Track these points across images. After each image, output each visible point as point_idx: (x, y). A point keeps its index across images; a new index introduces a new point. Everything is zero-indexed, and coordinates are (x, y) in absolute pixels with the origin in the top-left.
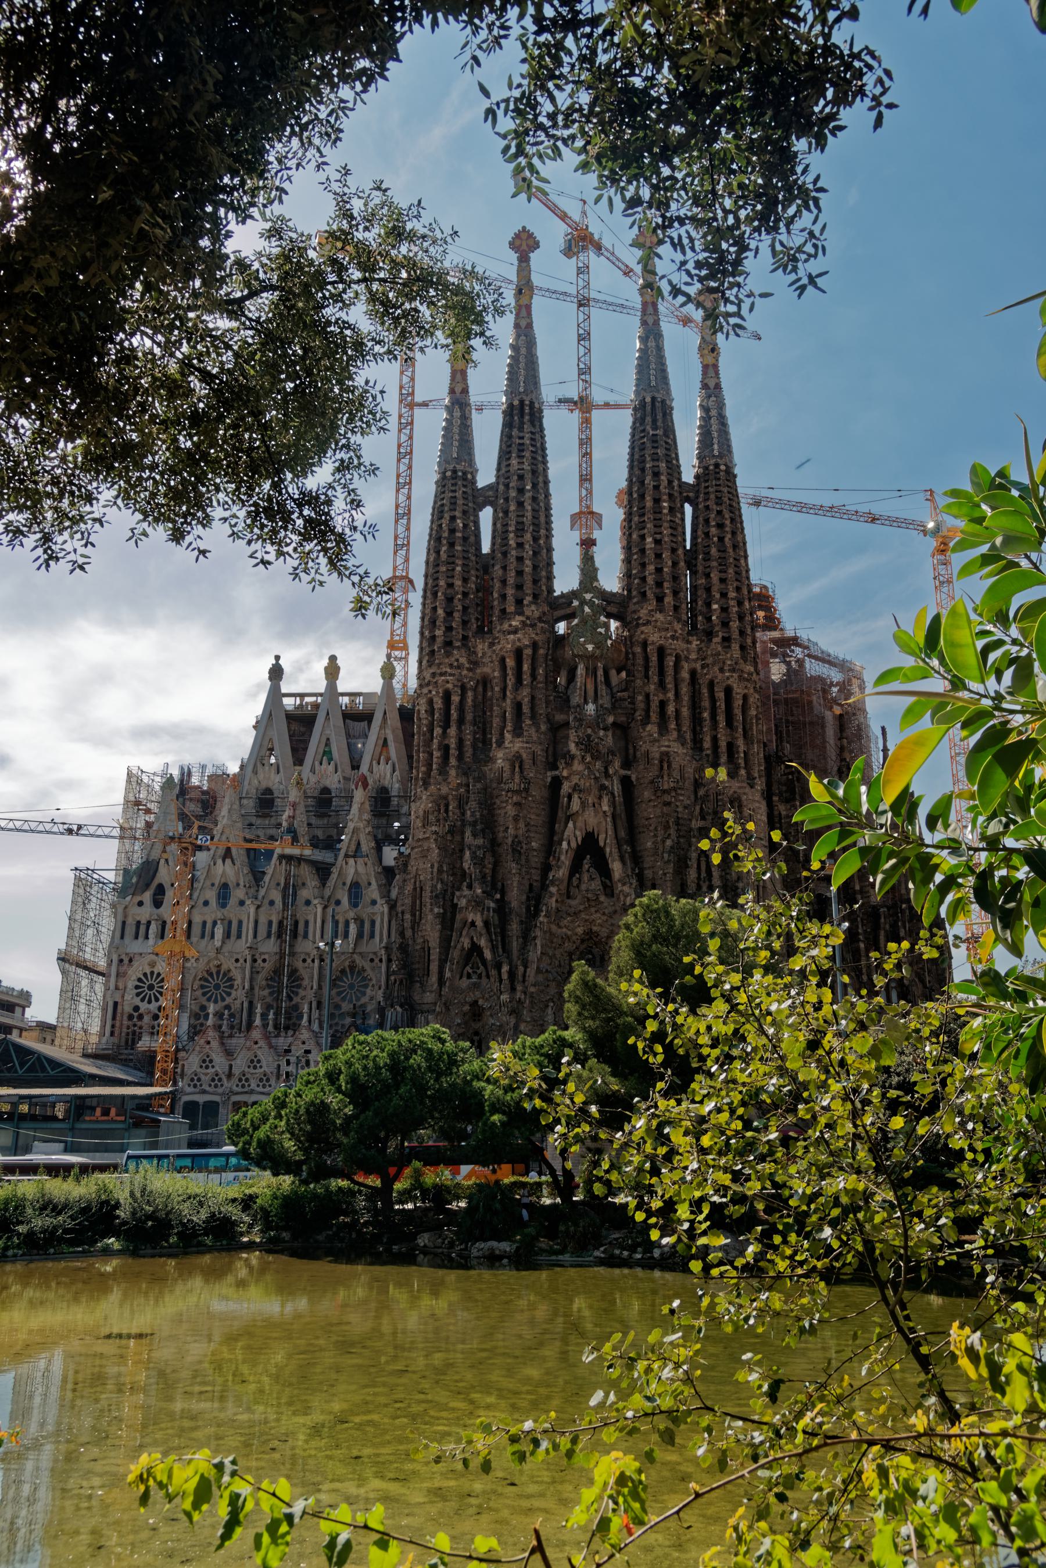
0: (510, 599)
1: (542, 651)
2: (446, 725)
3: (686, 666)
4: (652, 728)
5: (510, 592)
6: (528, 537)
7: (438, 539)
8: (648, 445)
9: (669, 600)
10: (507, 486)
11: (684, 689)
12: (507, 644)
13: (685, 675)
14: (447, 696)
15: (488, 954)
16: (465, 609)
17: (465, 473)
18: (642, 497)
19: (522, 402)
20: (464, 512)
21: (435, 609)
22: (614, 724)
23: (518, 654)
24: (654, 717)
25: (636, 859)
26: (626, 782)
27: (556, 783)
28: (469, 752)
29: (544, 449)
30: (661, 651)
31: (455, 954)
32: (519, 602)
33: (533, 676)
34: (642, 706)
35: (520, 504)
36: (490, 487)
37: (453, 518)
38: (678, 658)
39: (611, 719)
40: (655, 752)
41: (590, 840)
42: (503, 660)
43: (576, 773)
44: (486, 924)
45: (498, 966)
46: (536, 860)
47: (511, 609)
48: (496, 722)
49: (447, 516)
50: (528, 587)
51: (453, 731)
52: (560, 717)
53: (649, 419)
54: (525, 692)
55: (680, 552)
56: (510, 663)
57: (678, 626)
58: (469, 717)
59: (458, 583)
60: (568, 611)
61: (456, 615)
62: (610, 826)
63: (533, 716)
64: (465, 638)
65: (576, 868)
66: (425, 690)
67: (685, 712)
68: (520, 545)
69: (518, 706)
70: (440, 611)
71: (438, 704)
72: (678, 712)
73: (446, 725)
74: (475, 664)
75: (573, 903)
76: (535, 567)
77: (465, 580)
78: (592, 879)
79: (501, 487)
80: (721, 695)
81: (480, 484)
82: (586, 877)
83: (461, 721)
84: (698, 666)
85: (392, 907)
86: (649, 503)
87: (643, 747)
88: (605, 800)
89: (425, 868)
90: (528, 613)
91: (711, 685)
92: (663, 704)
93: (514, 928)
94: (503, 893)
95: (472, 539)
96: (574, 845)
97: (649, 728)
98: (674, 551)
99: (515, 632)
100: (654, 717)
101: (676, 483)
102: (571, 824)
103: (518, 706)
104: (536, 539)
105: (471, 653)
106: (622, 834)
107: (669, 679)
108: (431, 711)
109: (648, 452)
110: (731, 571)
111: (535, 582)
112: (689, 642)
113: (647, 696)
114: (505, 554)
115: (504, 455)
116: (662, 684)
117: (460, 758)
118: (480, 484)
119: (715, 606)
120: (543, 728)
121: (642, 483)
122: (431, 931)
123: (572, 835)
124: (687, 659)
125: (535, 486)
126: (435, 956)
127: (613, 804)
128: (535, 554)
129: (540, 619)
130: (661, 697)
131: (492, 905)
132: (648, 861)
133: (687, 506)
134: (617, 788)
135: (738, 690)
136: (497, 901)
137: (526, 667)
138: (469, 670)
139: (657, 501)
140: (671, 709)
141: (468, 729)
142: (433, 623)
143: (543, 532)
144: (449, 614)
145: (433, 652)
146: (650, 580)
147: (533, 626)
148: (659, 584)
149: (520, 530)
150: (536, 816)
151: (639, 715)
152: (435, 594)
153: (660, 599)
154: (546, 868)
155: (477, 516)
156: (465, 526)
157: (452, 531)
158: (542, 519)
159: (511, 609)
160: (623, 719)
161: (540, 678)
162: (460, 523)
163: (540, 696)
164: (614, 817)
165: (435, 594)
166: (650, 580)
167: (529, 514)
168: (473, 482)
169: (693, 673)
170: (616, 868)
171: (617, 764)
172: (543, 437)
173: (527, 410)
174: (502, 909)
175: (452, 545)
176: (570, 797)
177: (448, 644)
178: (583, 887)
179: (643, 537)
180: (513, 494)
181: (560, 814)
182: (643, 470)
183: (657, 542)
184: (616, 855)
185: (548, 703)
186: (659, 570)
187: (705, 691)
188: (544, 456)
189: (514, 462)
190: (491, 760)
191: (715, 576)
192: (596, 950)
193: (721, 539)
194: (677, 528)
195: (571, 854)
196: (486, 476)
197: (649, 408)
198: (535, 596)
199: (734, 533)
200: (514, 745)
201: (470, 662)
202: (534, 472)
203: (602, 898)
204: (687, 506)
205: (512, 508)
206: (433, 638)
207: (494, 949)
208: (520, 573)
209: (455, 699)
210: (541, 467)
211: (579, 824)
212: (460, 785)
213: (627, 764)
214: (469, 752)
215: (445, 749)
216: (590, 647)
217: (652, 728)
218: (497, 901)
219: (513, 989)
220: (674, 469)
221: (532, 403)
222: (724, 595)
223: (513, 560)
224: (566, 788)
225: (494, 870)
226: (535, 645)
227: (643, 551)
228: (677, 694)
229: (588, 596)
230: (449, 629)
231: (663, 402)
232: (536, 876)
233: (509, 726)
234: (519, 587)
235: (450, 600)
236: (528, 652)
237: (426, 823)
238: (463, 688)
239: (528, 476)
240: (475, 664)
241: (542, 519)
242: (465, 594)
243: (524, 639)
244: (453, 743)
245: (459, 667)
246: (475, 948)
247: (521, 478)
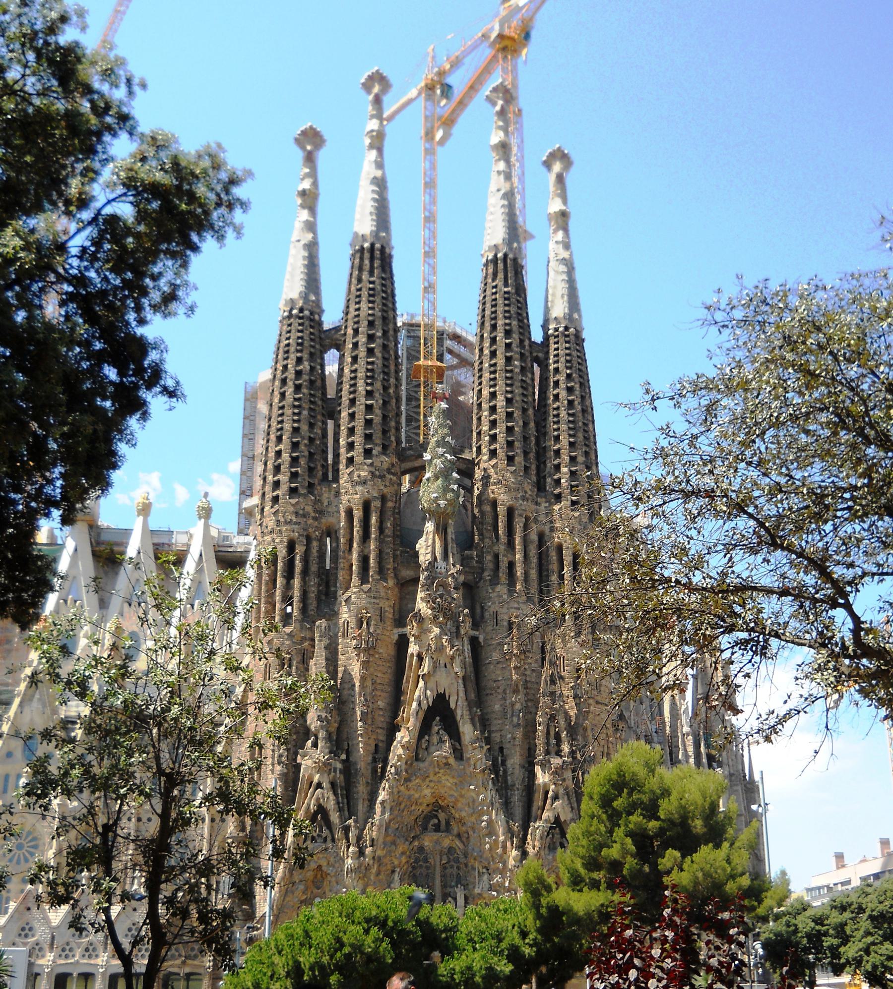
0: (359, 449)
1: (390, 504)
3: (534, 527)
4: (502, 589)
5: (358, 439)
6: (378, 385)
7: (284, 382)
8: (500, 302)
9: (519, 459)
10: (356, 332)
11: (533, 552)
13: (534, 537)
15: (335, 817)
16: (311, 455)
17: (312, 313)
18: (493, 354)
19: (372, 245)
20: (311, 355)
21: (279, 454)
22: (465, 584)
23: (366, 507)
24: (503, 576)
25: (483, 723)
26: (474, 641)
27: (402, 643)
28: (313, 604)
29: (393, 296)
30: (510, 512)
32: (368, 453)
33: (381, 529)
34: (490, 566)
35: (370, 352)
36: (337, 329)
37: (299, 360)
38: (527, 519)
39: (462, 578)
42: (349, 513)
44: (333, 785)
45: (347, 829)
46: (381, 719)
47: (359, 459)
48: (341, 575)
49: (293, 357)
50: (378, 437)
51: (297, 582)
52: (407, 573)
53: (501, 275)
55: (531, 412)
56: (357, 514)
57: (528, 488)
58: (314, 568)
59: (304, 428)
60: (417, 464)
61: (302, 462)
62: (461, 688)
63: (381, 571)
64: (311, 486)
65: (425, 729)
66: (268, 538)
67: (534, 574)
68: (369, 394)
70: (286, 456)
71: (282, 552)
72: (526, 574)
75: (421, 765)
76: (385, 417)
77: (311, 426)
78: (441, 741)
79: (350, 331)
80: (568, 559)
81: (326, 326)
82: (435, 739)
83: (305, 572)
84: (547, 529)
86: (500, 361)
87: (492, 607)
88: (458, 660)
90: (377, 463)
91: (560, 548)
93: (361, 789)
94: (348, 753)
95: (319, 383)
96: (425, 706)
97: (499, 588)
98: (524, 410)
99: (364, 483)
100: (503, 576)
101: (527, 343)
102: (421, 683)
104: (385, 388)
105: (318, 501)
106: (473, 696)
109: (500, 309)
110: (580, 435)
111: (385, 432)
112: (537, 504)
113: (496, 556)
114: (353, 402)
115: (353, 298)
116: (511, 544)
117: (304, 610)
118: (326, 326)
119: (564, 470)
120: (391, 583)
121: (493, 340)
124: (536, 521)
125: (385, 333)
127: (464, 664)
128: (385, 403)
129: (389, 471)
130: (510, 557)
131: (339, 766)
132: (496, 724)
133: (535, 365)
134: (467, 647)
136: (343, 762)
137: (374, 520)
138: (315, 519)
139: (508, 360)
140: (519, 571)
141: (313, 581)
142: (277, 469)
143: (392, 381)
144: (294, 461)
145: (276, 500)
147: (382, 477)
148: (510, 444)
149: (371, 377)
151: (487, 575)
152: (279, 439)
153: (510, 460)
154: (393, 729)
155: (323, 359)
156: (312, 369)
157: (298, 374)
158: (392, 368)
159: (359, 459)
160: (470, 577)
161: (388, 532)
163: (388, 550)
164: (464, 678)
165: (279, 439)
167: (379, 362)
168: (320, 323)
169: (541, 536)
170: (468, 731)
171: (468, 624)
172: (393, 284)
173: (377, 253)
174: (348, 769)
175: (298, 388)
176: (420, 658)
177: (293, 491)
178: (432, 748)
179: (493, 395)
180: (362, 339)
181: (409, 675)
182: (494, 327)
183: (509, 401)
184: (467, 717)
185: (395, 557)
186: (510, 430)
187: (553, 555)
188: (394, 303)
189: (364, 305)
190: (336, 614)
192: (442, 816)
193: (571, 403)
194: (526, 387)
195: (421, 715)
196: (331, 317)
197: (501, 265)
198: (385, 448)
199: (583, 398)
201: (316, 511)
202: (384, 319)
203: (452, 761)
204: (535, 365)
205: (362, 352)
206: (277, 485)
207: (340, 810)
208: (368, 423)
209: (299, 550)
210: (391, 314)
211: (432, 684)
212: (304, 639)
213: (475, 625)
214: (313, 604)
216: (442, 503)
217: (502, 589)
218: (343, 762)
219: (361, 853)
220: (525, 328)
221: (383, 249)
222: (573, 459)
223: (363, 407)
224: (413, 649)
225: (339, 729)
226: (383, 499)
227: (493, 409)
228: (526, 556)
229: (440, 450)
230: (294, 476)
231: (515, 260)
232: (382, 736)
233: (355, 579)
234: (368, 437)
235: (295, 446)
238: (309, 539)
239: (378, 323)
240: (321, 513)
241: (392, 368)
242: (311, 440)
244: (297, 594)
245: (304, 516)
246: (321, 810)
247: (371, 324)
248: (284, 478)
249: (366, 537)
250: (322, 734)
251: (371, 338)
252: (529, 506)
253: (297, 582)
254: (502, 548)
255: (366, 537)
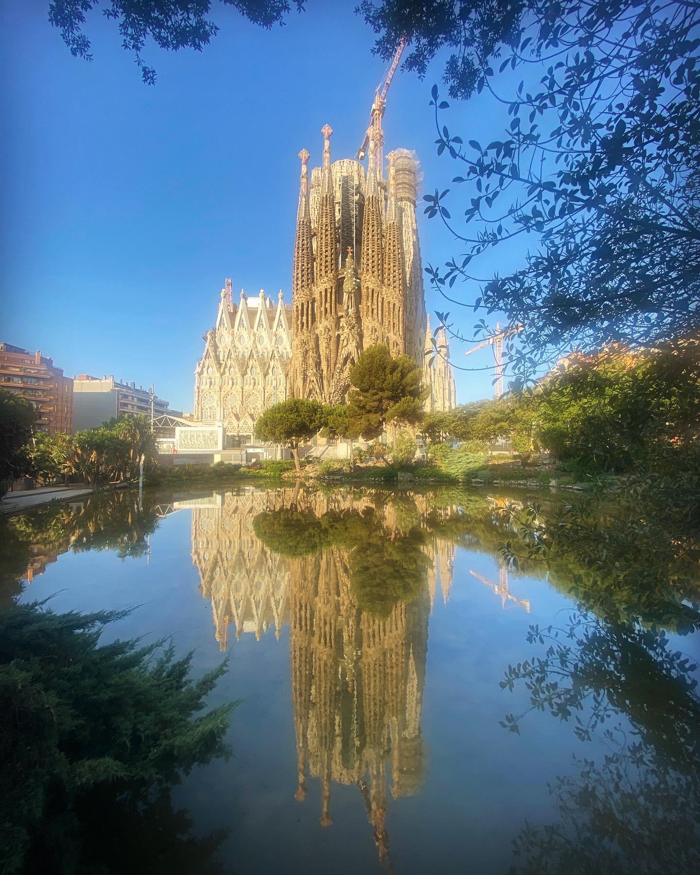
0: (323, 271)
2: (302, 316)
5: (323, 268)
6: (329, 248)
12: (322, 288)
13: (380, 300)
14: (303, 304)
23: (326, 290)
27: (339, 336)
31: (307, 390)
32: (326, 272)
35: (326, 235)
40: (370, 327)
41: (349, 354)
43: (345, 333)
47: (323, 274)
51: (305, 318)
54: (328, 305)
56: (323, 294)
58: (310, 313)
67: (380, 312)
69: (326, 309)
73: (302, 316)
74: (311, 294)
80: (392, 307)
85: (287, 376)
89: (298, 363)
92: (373, 310)
100: (370, 314)
103: (326, 309)
107: (375, 301)
108: (297, 311)
117: (307, 327)
122: (300, 382)
123: (343, 353)
126: (301, 390)
135: (397, 305)
140: (375, 311)
144: (303, 276)
146: (370, 265)
149: (326, 245)
150: (333, 346)
157: (303, 245)
159: (323, 274)
162: (305, 242)
166: (370, 265)
177: (303, 286)
186: (373, 262)
191: (392, 265)
200: (325, 323)
208: (326, 261)
209: (305, 306)
215: (302, 324)
217: (370, 318)
224: (342, 338)
230: (303, 281)
234: (326, 267)
235: (303, 271)
236: (329, 290)
237: (297, 348)
243: (328, 286)
248: (299, 282)
249: (326, 302)
250: (314, 365)
251: (326, 230)
252: (378, 289)
253: (305, 318)
254: (369, 304)
255: (326, 302)
